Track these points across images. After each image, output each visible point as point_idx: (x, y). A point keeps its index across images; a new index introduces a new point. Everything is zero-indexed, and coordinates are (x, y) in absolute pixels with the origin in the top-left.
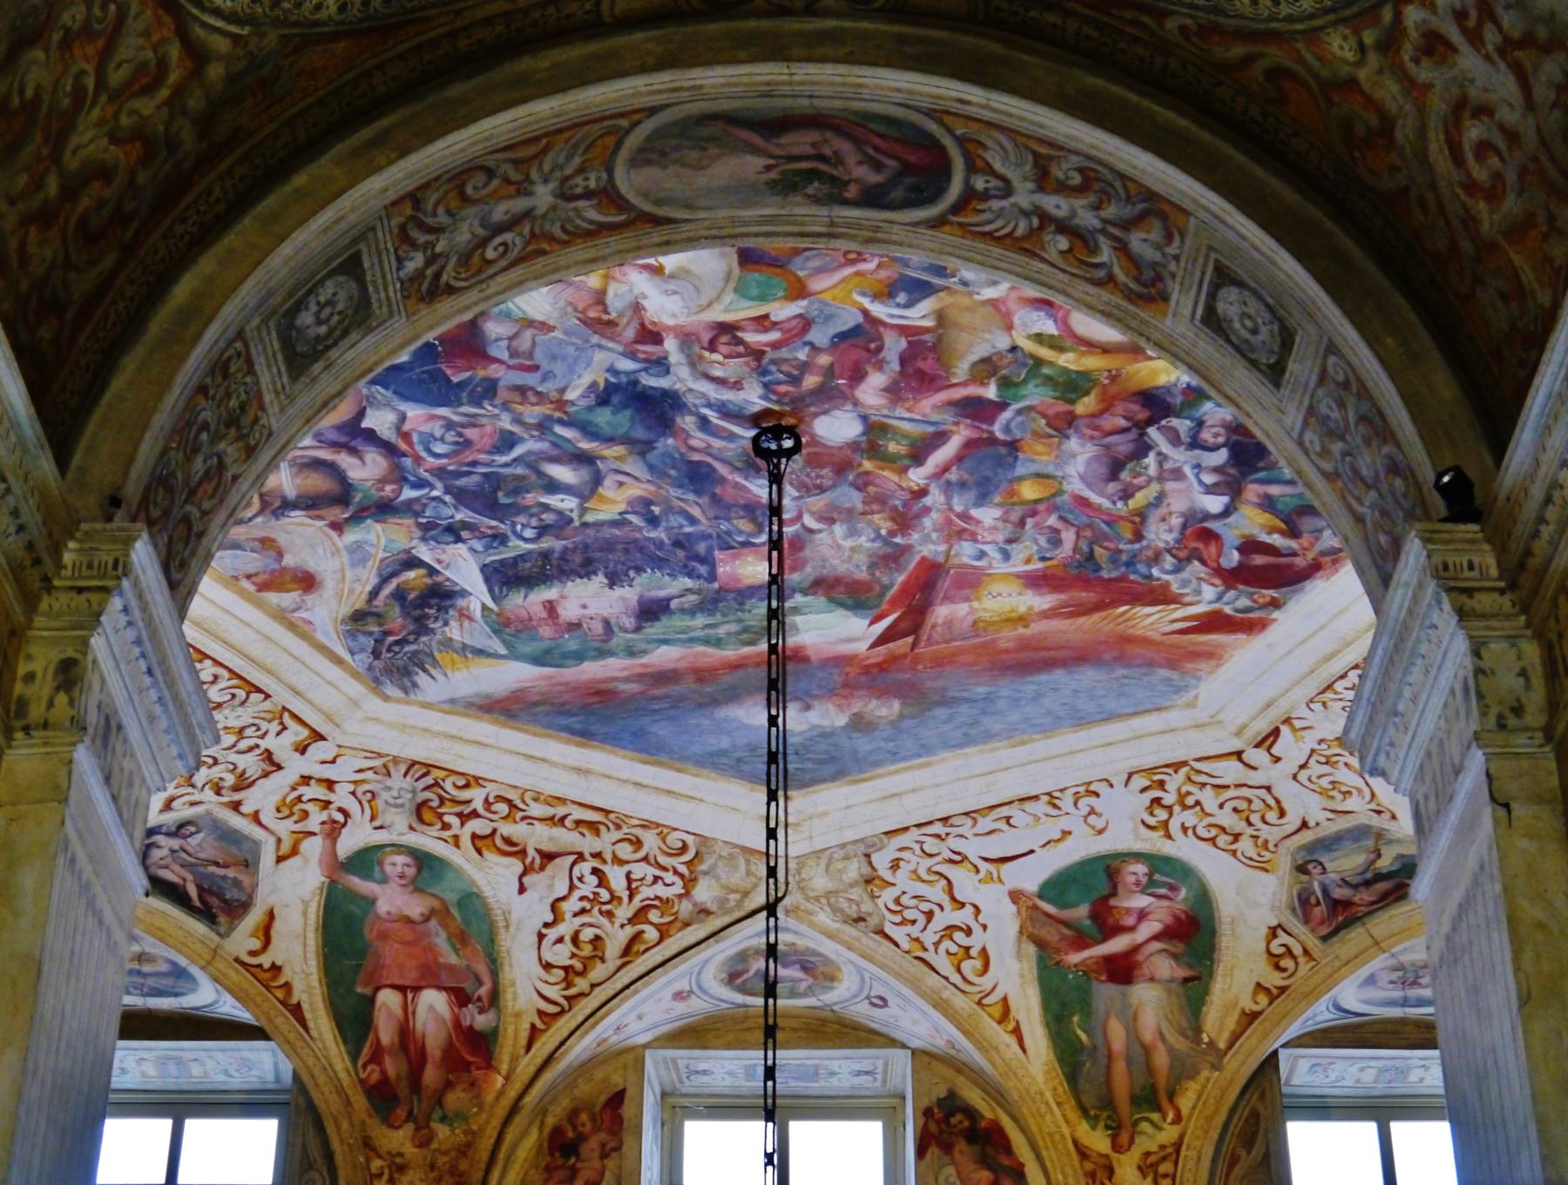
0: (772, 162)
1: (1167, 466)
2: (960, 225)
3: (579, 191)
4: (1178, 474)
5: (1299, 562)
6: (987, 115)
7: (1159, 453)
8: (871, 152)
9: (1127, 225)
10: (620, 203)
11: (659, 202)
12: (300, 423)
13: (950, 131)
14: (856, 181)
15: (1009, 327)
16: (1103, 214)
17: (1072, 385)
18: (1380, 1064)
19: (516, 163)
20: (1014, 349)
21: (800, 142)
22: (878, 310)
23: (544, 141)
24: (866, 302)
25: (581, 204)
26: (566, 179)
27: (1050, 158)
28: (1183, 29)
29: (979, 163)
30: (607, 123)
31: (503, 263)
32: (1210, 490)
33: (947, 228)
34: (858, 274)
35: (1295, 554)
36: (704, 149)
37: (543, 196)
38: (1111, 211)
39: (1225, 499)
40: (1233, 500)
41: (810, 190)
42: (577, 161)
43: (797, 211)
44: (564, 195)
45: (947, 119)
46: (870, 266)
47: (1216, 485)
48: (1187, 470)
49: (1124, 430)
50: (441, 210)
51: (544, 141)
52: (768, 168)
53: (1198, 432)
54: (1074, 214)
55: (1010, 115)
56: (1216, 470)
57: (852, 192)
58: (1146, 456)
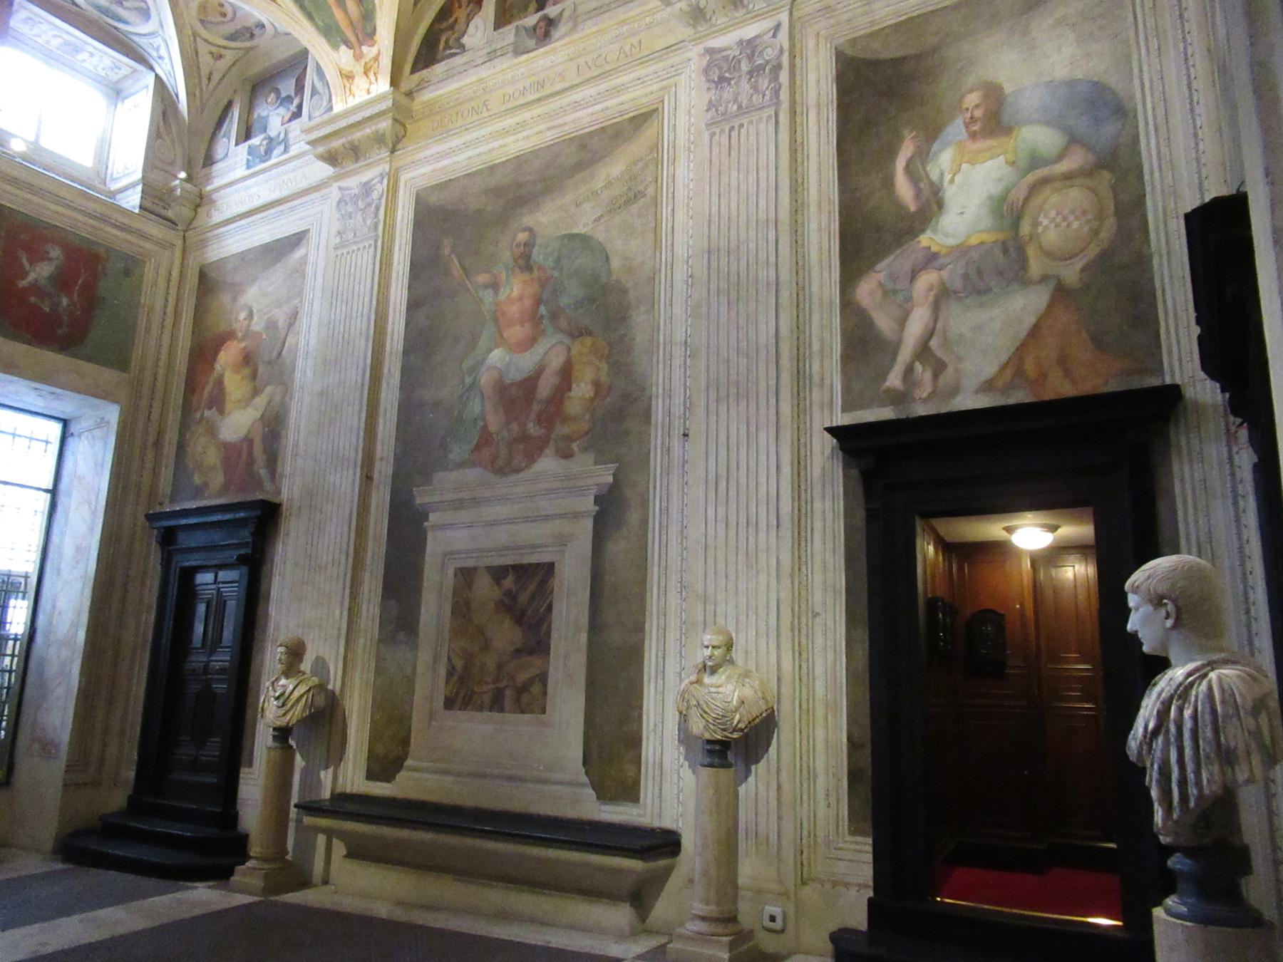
18: (65, 36)
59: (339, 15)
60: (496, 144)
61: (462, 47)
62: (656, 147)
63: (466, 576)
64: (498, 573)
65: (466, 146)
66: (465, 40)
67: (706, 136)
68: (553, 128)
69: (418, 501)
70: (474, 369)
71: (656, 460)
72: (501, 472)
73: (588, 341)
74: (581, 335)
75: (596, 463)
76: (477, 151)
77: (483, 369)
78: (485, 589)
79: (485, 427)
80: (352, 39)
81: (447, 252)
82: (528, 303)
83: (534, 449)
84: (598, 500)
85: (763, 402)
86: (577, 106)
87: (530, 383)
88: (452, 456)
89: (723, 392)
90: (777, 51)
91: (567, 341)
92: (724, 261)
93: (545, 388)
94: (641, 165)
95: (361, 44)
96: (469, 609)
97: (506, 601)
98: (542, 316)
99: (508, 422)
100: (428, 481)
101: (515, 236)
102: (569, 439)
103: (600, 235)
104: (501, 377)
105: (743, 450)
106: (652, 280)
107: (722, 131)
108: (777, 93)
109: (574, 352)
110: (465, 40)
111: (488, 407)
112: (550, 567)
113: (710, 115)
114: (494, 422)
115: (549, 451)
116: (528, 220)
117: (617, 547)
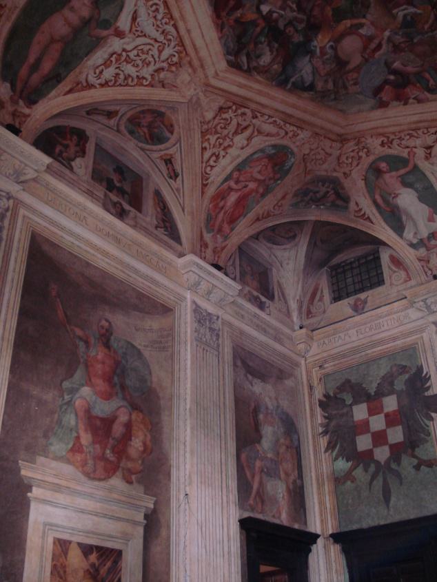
1: (288, 9)
4: (282, 8)
5: (224, 14)
7: (295, 11)
15: (372, 23)
17: (339, 15)
20: (364, 17)
22: (412, 10)
24: (419, 11)
32: (270, 12)
34: (427, 22)
35: (228, 14)
39: (264, 13)
40: (262, 16)
46: (426, 27)
47: (272, 15)
48: (283, 13)
49: (311, 10)
53: (294, 27)
56: (276, 21)
58: (297, 6)
59: (24, 72)
60: (92, 251)
61: (71, 169)
62: (172, 329)
63: (62, 546)
64: (87, 550)
65: (71, 234)
66: (73, 164)
67: (195, 343)
68: (124, 272)
69: (23, 472)
70: (73, 391)
71: (174, 504)
72: (87, 475)
73: (141, 415)
74: (137, 409)
75: (145, 494)
76: (77, 243)
77: (77, 395)
78: (75, 559)
79: (78, 438)
80: (19, 88)
81: (54, 293)
82: (108, 369)
83: (111, 470)
84: (146, 517)
85: (217, 491)
86: (136, 271)
87: (109, 422)
88: (52, 448)
89: (203, 480)
90: (217, 328)
91: (130, 408)
92: (202, 413)
93: (118, 430)
94: (165, 333)
95: (21, 97)
96: (65, 572)
97: (92, 571)
98: (116, 384)
99: (94, 442)
100: (33, 461)
101: (100, 320)
102: (130, 472)
103: (146, 353)
104: (89, 408)
105: (211, 513)
106: (171, 399)
107: (200, 347)
108: (218, 345)
109: (134, 417)
110: (73, 164)
111: (81, 427)
112: (119, 553)
113: (196, 334)
114: (86, 439)
115: (119, 473)
116: (108, 315)
117: (156, 549)
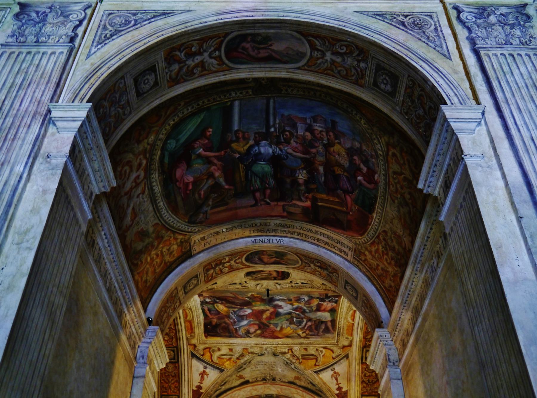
0: (270, 47)
2: (220, 38)
3: (320, 53)
6: (218, 74)
8: (245, 53)
9: (180, 69)
10: (309, 42)
11: (300, 39)
12: (402, 63)
13: (227, 65)
14: (248, 42)
16: (186, 66)
19: (332, 71)
21: (263, 54)
23: (325, 72)
25: (319, 48)
26: (322, 58)
27: (202, 71)
28: (180, 105)
29: (218, 59)
30: (310, 69)
31: (343, 43)
33: (223, 35)
36: (287, 53)
37: (329, 56)
38: (185, 69)
41: (260, 38)
42: (319, 62)
43: (264, 31)
44: (324, 54)
45: (228, 68)
50: (353, 73)
51: (325, 72)
52: (271, 45)
54: (193, 61)
55: (214, 77)
57: (249, 38)
